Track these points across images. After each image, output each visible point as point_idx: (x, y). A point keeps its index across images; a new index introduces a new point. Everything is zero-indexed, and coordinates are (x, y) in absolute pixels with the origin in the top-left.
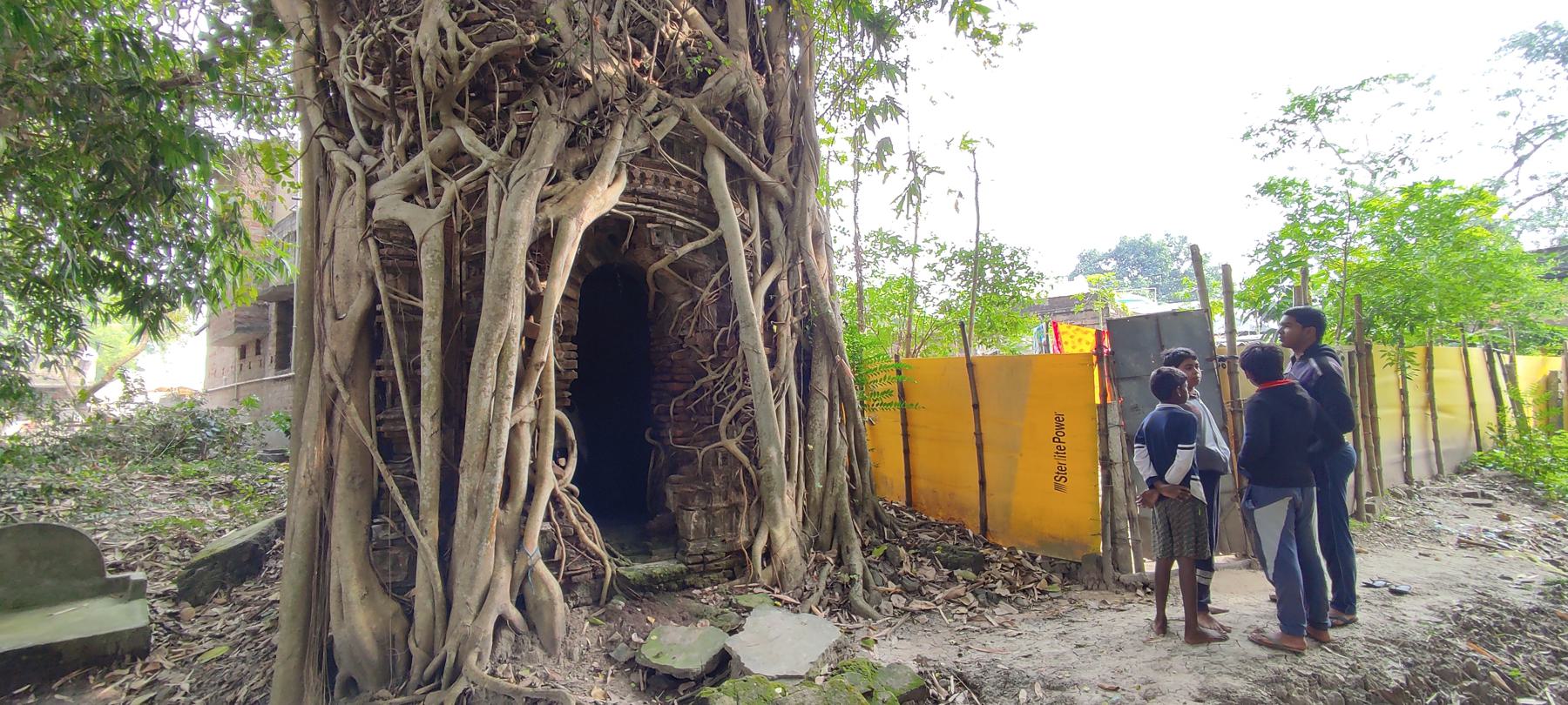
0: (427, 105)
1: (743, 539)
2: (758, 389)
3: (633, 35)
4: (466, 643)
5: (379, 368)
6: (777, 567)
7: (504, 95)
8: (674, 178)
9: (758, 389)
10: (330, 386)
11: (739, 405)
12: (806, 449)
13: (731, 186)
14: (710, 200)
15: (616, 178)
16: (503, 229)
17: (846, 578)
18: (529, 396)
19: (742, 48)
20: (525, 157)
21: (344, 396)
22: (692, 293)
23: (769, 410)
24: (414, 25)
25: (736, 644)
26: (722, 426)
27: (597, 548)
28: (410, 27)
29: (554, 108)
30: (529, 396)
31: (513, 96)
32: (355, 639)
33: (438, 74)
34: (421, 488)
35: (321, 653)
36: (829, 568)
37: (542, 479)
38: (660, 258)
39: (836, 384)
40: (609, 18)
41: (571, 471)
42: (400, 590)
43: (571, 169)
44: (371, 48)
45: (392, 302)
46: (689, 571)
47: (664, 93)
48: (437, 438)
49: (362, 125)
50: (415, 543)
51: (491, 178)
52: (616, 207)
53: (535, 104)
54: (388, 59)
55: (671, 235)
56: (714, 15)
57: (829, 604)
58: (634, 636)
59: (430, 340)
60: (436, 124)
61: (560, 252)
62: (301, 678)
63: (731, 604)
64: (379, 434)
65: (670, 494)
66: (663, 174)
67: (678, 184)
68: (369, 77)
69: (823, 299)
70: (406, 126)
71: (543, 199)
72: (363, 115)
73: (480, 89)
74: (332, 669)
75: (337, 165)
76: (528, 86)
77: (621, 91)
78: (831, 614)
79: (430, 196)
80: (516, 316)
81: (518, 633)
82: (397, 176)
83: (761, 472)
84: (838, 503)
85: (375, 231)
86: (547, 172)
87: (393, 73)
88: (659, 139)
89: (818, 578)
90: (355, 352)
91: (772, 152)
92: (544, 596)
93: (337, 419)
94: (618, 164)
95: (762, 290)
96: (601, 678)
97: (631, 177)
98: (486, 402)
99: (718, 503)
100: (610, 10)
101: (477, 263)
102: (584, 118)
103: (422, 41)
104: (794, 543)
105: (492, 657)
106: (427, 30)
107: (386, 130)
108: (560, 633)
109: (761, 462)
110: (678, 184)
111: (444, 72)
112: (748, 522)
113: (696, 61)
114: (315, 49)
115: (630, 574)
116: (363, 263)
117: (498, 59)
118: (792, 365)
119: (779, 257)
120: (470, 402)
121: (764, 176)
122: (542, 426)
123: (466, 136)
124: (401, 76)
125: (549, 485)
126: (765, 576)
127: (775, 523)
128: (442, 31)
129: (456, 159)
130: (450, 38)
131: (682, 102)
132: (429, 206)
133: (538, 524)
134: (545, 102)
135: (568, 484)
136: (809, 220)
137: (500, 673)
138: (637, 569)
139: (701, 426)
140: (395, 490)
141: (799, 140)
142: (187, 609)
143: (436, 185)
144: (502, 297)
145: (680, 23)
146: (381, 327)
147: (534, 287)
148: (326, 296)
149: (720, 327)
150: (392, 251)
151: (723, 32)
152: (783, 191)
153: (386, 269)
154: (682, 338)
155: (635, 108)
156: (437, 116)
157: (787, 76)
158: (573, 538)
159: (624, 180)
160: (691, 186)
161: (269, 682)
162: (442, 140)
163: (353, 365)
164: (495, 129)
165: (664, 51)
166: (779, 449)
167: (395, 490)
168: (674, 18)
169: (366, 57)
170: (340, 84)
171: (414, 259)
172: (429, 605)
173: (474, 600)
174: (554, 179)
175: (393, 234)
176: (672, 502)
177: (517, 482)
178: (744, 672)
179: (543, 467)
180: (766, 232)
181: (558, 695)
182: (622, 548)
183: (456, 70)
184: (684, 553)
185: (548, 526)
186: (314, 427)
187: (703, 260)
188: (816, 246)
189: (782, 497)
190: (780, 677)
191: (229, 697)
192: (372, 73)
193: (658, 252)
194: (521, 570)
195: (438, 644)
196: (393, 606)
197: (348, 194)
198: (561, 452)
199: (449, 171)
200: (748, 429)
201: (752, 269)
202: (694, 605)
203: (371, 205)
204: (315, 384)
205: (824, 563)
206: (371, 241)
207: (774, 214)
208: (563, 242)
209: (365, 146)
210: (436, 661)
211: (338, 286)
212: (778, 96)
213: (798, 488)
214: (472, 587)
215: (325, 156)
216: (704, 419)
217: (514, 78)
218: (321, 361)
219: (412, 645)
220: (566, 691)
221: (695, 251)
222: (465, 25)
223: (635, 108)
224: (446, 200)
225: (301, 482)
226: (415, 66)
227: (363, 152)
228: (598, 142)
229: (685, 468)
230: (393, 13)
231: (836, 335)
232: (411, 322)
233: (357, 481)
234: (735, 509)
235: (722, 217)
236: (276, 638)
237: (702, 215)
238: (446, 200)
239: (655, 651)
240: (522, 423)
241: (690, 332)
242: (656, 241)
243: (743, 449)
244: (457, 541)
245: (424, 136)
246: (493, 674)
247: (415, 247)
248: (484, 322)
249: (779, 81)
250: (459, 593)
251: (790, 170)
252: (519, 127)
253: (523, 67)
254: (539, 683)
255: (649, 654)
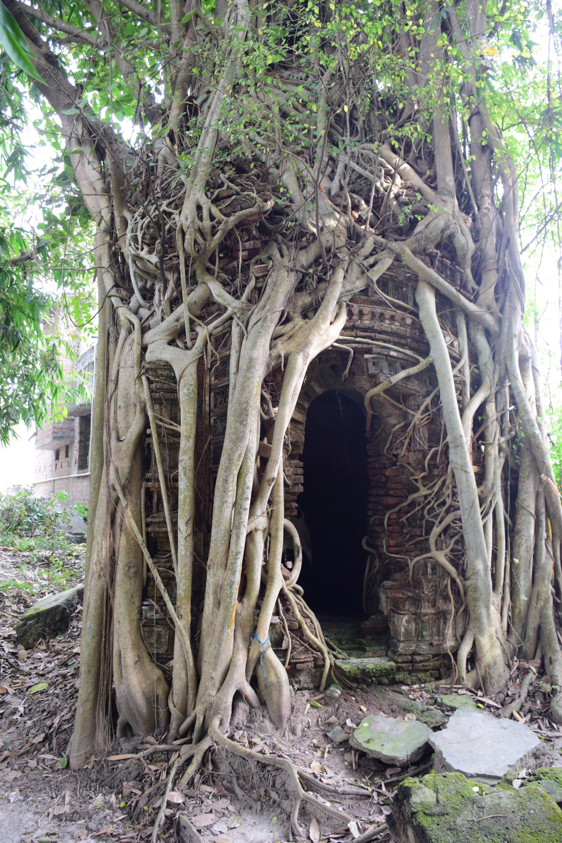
0: (187, 266)
1: (449, 643)
4: (212, 709)
5: (148, 480)
6: (481, 672)
7: (246, 253)
8: (388, 313)
10: (113, 494)
11: (448, 519)
12: (512, 563)
13: (441, 317)
14: (422, 331)
15: (337, 316)
16: (243, 365)
17: (547, 688)
18: (262, 507)
19: (450, 193)
20: (261, 303)
21: (123, 502)
22: (405, 415)
23: (476, 525)
24: (178, 206)
25: (439, 740)
26: (432, 538)
28: (176, 207)
29: (286, 260)
31: (253, 253)
32: (130, 696)
33: (196, 242)
34: (178, 580)
35: (107, 700)
36: (531, 677)
37: (272, 579)
38: (376, 385)
39: (542, 502)
40: (332, 179)
42: (162, 659)
43: (299, 310)
44: (148, 227)
45: (158, 427)
46: (399, 669)
47: (380, 238)
48: (190, 540)
49: (140, 284)
50: (173, 623)
51: (234, 323)
52: (337, 341)
53: (270, 258)
54: (160, 235)
55: (385, 364)
56: (423, 165)
57: (530, 711)
58: (348, 722)
60: (193, 281)
61: (289, 383)
62: (94, 718)
63: (436, 702)
64: (148, 534)
65: (383, 597)
66: (378, 310)
67: (392, 318)
68: (146, 248)
69: (529, 420)
70: (171, 285)
71: (275, 338)
72: (141, 277)
73: (228, 249)
74: (115, 715)
75: (122, 318)
76: (265, 244)
77: (342, 240)
79: (188, 339)
80: (252, 439)
81: (251, 707)
82: (164, 325)
83: (468, 583)
84: (542, 616)
85: (147, 370)
86: (278, 315)
87: (163, 245)
88: (375, 279)
89: (520, 685)
91: (479, 283)
92: (273, 678)
93: (118, 521)
94: (339, 303)
96: (319, 753)
97: (350, 314)
99: (427, 609)
100: (333, 172)
101: (222, 393)
102: (310, 267)
103: (185, 217)
104: (498, 651)
105: (231, 724)
106: (188, 208)
107: (157, 287)
108: (286, 711)
109: (469, 574)
110: (392, 318)
111: (200, 240)
112: (455, 628)
113: (407, 210)
114: (110, 231)
115: (346, 667)
116: (138, 396)
117: (241, 225)
118: (499, 483)
120: (216, 511)
121: (471, 307)
122: (273, 533)
123: (217, 290)
124: (169, 245)
125: (278, 584)
126: (468, 679)
127: (481, 631)
128: (199, 208)
129: (208, 309)
130: (205, 213)
131: (394, 245)
132: (187, 348)
133: (268, 617)
134: (278, 256)
135: (294, 584)
136: (515, 345)
137: (237, 737)
138: (352, 663)
139: (412, 537)
141: (505, 271)
142: (22, 652)
143: (192, 330)
144: (241, 423)
145: (393, 177)
146: (150, 446)
147: (267, 412)
148: (112, 422)
149: (430, 447)
150: (159, 385)
151: (432, 181)
152: (490, 319)
153: (155, 401)
154: (396, 456)
155: (353, 254)
156: (194, 273)
157: (492, 214)
158: (298, 632)
160: (403, 319)
161: (73, 716)
162: (198, 293)
166: (485, 562)
168: (388, 174)
169: (144, 234)
170: (125, 255)
171: (175, 391)
172: (183, 675)
173: (218, 675)
174: (285, 319)
175: (160, 372)
176: (385, 605)
177: (252, 580)
178: (446, 767)
179: (273, 569)
180: (474, 357)
181: (283, 763)
183: (209, 237)
184: (395, 652)
186: (102, 526)
187: (415, 386)
189: (488, 608)
190: (478, 776)
191: (48, 723)
192: (148, 245)
193: (374, 380)
194: (254, 655)
195: (190, 709)
196: (157, 673)
197: (129, 341)
198: (289, 555)
200: (457, 542)
201: (461, 393)
202: (402, 699)
203: (144, 349)
204: (103, 491)
205: (527, 671)
208: (292, 374)
209: (142, 302)
210: (188, 720)
212: (483, 232)
213: (503, 599)
214: (216, 665)
215: (114, 310)
217: (254, 238)
218: (108, 474)
219: (171, 705)
220: (289, 760)
221: (408, 378)
222: (216, 201)
223: (353, 254)
224: (199, 342)
225: (94, 568)
226: (178, 237)
227: (140, 306)
228: (322, 286)
229: (397, 576)
230: (165, 197)
231: (543, 455)
232: (171, 442)
233: (132, 570)
234: (442, 615)
235: (432, 346)
236: (78, 683)
237: (414, 345)
238: (199, 342)
242: (372, 370)
243: (452, 561)
244: (205, 625)
245: (184, 292)
246: (232, 737)
247: (175, 382)
248: (227, 444)
249: (485, 220)
250: (206, 668)
251: (497, 300)
252: (257, 278)
253: (262, 229)
254: (268, 751)
255: (362, 737)
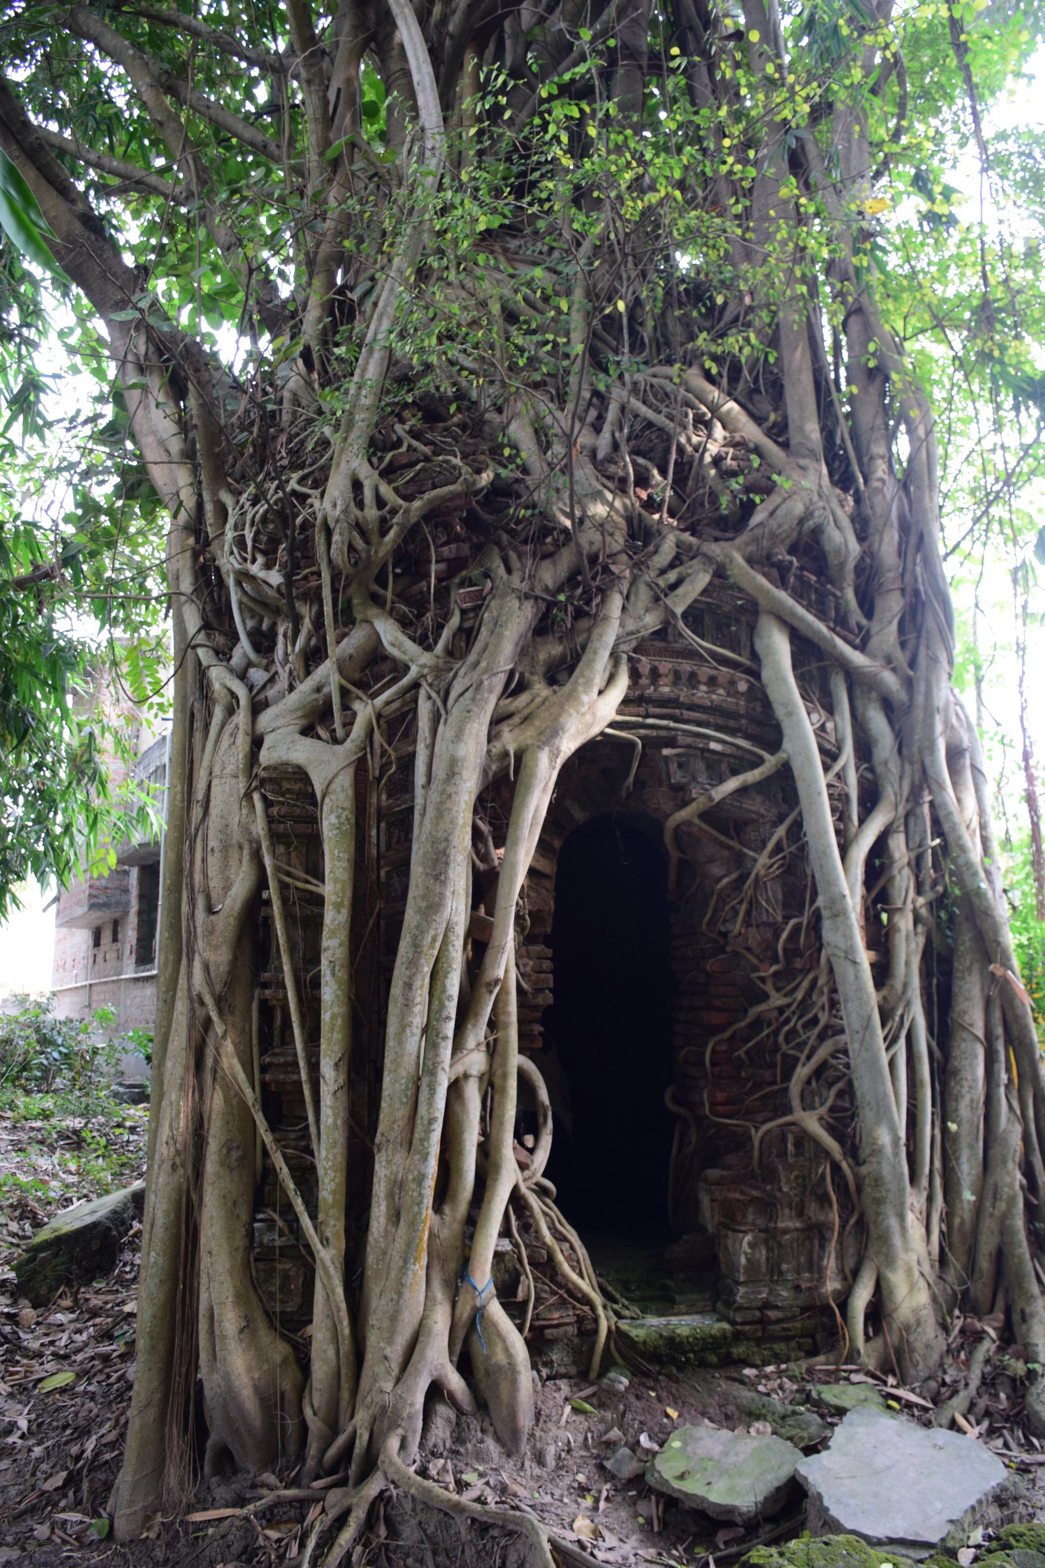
0: (335, 591)
1: (832, 1285)
2: (856, 1025)
3: (635, 452)
4: (386, 1419)
5: (265, 985)
6: (893, 1339)
7: (442, 566)
8: (705, 672)
9: (856, 1025)
10: (200, 1012)
11: (823, 1052)
12: (945, 1130)
13: (800, 678)
14: (767, 704)
15: (611, 679)
16: (440, 770)
17: (1019, 1368)
18: (477, 1034)
19: (812, 454)
20: (472, 657)
21: (219, 1028)
22: (738, 860)
23: (875, 1060)
24: (320, 482)
25: (819, 1473)
26: (795, 1087)
27: (584, 1285)
28: (316, 485)
29: (515, 580)
30: (477, 1034)
31: (455, 566)
32: (230, 1394)
33: (351, 548)
34: (321, 1172)
36: (987, 1347)
37: (497, 1168)
38: (684, 804)
39: (997, 1015)
40: (597, 428)
41: (541, 1158)
42: (291, 1323)
43: (540, 669)
44: (264, 519)
45: (283, 887)
46: (738, 1337)
47: (687, 537)
48: (342, 1095)
49: (250, 624)
50: (311, 1253)
51: (422, 694)
52: (612, 725)
53: (487, 575)
54: (286, 534)
55: (700, 766)
56: (764, 405)
57: (988, 1414)
58: (644, 1439)
59: (333, 944)
60: (346, 619)
61: (524, 805)
62: (162, 1438)
63: (808, 1399)
64: (264, 1085)
65: (705, 1200)
66: (687, 666)
67: (712, 682)
68: (260, 560)
69: (969, 865)
70: (307, 624)
71: (498, 720)
72: (251, 610)
73: (409, 559)
74: (202, 1432)
75: (217, 686)
76: (478, 549)
77: (618, 541)
78: (992, 1432)
79: (337, 725)
80: (457, 907)
81: (460, 1411)
82: (293, 699)
83: (864, 1170)
84: (1004, 1230)
85: (263, 782)
86: (502, 678)
87: (291, 551)
88: (679, 611)
89: (967, 1363)
90: (234, 963)
91: (869, 614)
92: (500, 1357)
93: (209, 1062)
94: (615, 656)
95: (860, 851)
96: (589, 1502)
97: (635, 675)
98: (413, 1042)
99: (788, 1222)
100: (601, 418)
101: (401, 824)
102: (560, 590)
103: (331, 503)
104: (923, 1297)
105: (421, 1446)
106: (337, 486)
107: (281, 630)
108: (525, 1420)
109: (865, 1152)
110: (712, 682)
111: (359, 544)
112: (841, 1257)
113: (736, 484)
114: (195, 527)
115: (637, 1333)
116: (246, 829)
117: (434, 515)
118: (916, 982)
119: (889, 793)
120: (391, 1043)
121: (857, 658)
122: (497, 1081)
123: (389, 633)
124: (302, 555)
125: (509, 1177)
126: (869, 1354)
127: (890, 1260)
128: (357, 486)
129: (373, 668)
130: (368, 494)
131: (715, 549)
132: (336, 741)
133: (490, 1241)
134: (502, 571)
135: (538, 1177)
136: (939, 727)
137: (433, 1472)
138: (648, 1326)
139: (758, 1086)
140: (284, 1173)
141: (916, 593)
142: (28, 1313)
143: (346, 707)
144: (436, 878)
145: (708, 426)
146: (267, 923)
147: (485, 857)
148: (198, 877)
149: (787, 918)
150: (284, 810)
151: (779, 432)
152: (890, 680)
153: (275, 837)
154: (725, 935)
155: (639, 566)
156: (349, 603)
157: (890, 489)
158: (546, 1267)
159: (622, 683)
160: (733, 683)
161: (122, 1436)
162: (356, 640)
163: (230, 982)
164: (429, 618)
165: (685, 472)
166: (893, 1130)
167: (284, 1173)
168: (700, 421)
169: (257, 533)
170: (224, 570)
171: (313, 821)
172: (331, 1353)
173: (395, 1352)
174: (516, 686)
175: (286, 785)
176: (709, 1215)
177: (460, 1171)
178: (833, 1526)
179: (498, 1149)
180: (864, 750)
181: (521, 1522)
182: (626, 1288)
183: (374, 538)
184: (729, 1304)
185: (506, 1245)
186: (179, 1071)
187: (756, 805)
188: (955, 771)
189: (901, 1217)
190: (892, 1541)
191: (74, 1450)
192: (264, 553)
193: (681, 796)
194: (465, 1312)
195: (343, 1417)
196: (279, 1350)
197: (229, 728)
198: (528, 1124)
199: (363, 685)
200: (840, 1095)
201: (841, 815)
202: (745, 1394)
203: (257, 742)
204: (181, 1006)
205: (979, 1337)
206: (256, 796)
207: (878, 722)
208: (529, 788)
209: (253, 656)
210: (341, 1440)
211: (214, 862)
212: (875, 523)
213: (930, 1199)
214: (392, 1332)
215: (202, 672)
216: (761, 1074)
217: (456, 539)
218: (190, 975)
219: (308, 1412)
220: (533, 1516)
221: (743, 791)
222: (388, 473)
223: (639, 566)
224: (358, 729)
225: (164, 1151)
226: (320, 539)
227: (250, 664)
228: (584, 623)
229: (732, 1159)
230: (294, 467)
231: (996, 928)
232: (307, 913)
233: (235, 1154)
234: (817, 1232)
235: (787, 731)
236: (132, 1370)
237: (753, 729)
238: (358, 729)
239: (680, 1466)
240: (466, 1076)
241: (737, 927)
242: (677, 777)
243: (831, 1130)
244: (371, 1258)
245: (330, 638)
246: (423, 1472)
247: (315, 804)
248: (411, 917)
249: (878, 500)
250: (373, 1339)
251: (903, 645)
252: (463, 612)
253: (472, 522)
254: (491, 1498)
255: (668, 1468)
